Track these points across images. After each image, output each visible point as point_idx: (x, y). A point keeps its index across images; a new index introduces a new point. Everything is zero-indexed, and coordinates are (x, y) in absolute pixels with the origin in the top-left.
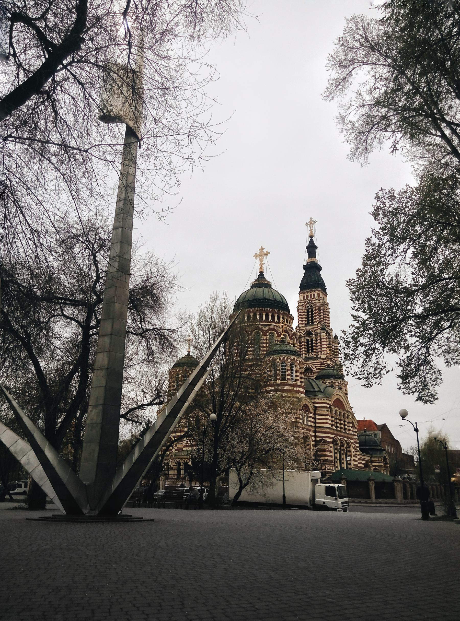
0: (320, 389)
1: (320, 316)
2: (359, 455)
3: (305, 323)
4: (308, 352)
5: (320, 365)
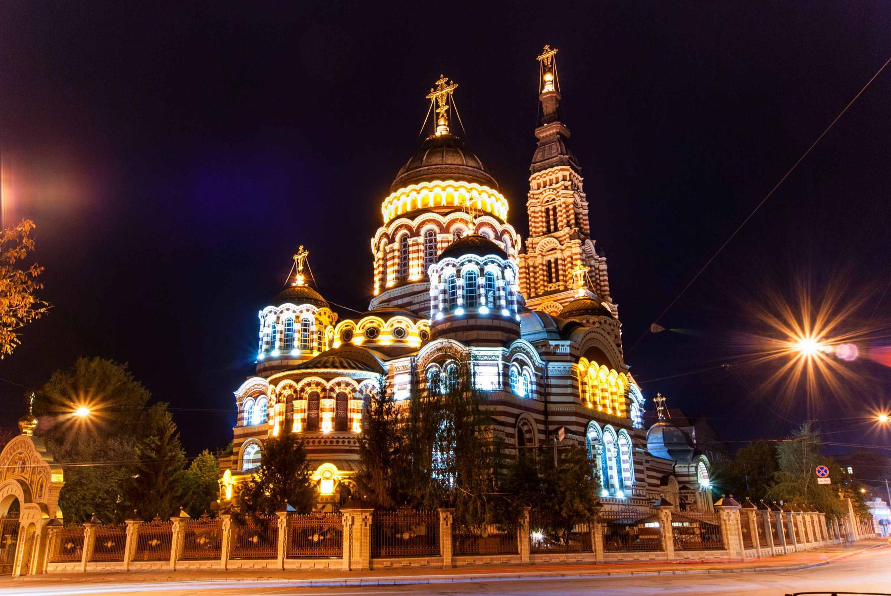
1: (567, 211)
3: (543, 232)
4: (550, 282)
5: (571, 302)
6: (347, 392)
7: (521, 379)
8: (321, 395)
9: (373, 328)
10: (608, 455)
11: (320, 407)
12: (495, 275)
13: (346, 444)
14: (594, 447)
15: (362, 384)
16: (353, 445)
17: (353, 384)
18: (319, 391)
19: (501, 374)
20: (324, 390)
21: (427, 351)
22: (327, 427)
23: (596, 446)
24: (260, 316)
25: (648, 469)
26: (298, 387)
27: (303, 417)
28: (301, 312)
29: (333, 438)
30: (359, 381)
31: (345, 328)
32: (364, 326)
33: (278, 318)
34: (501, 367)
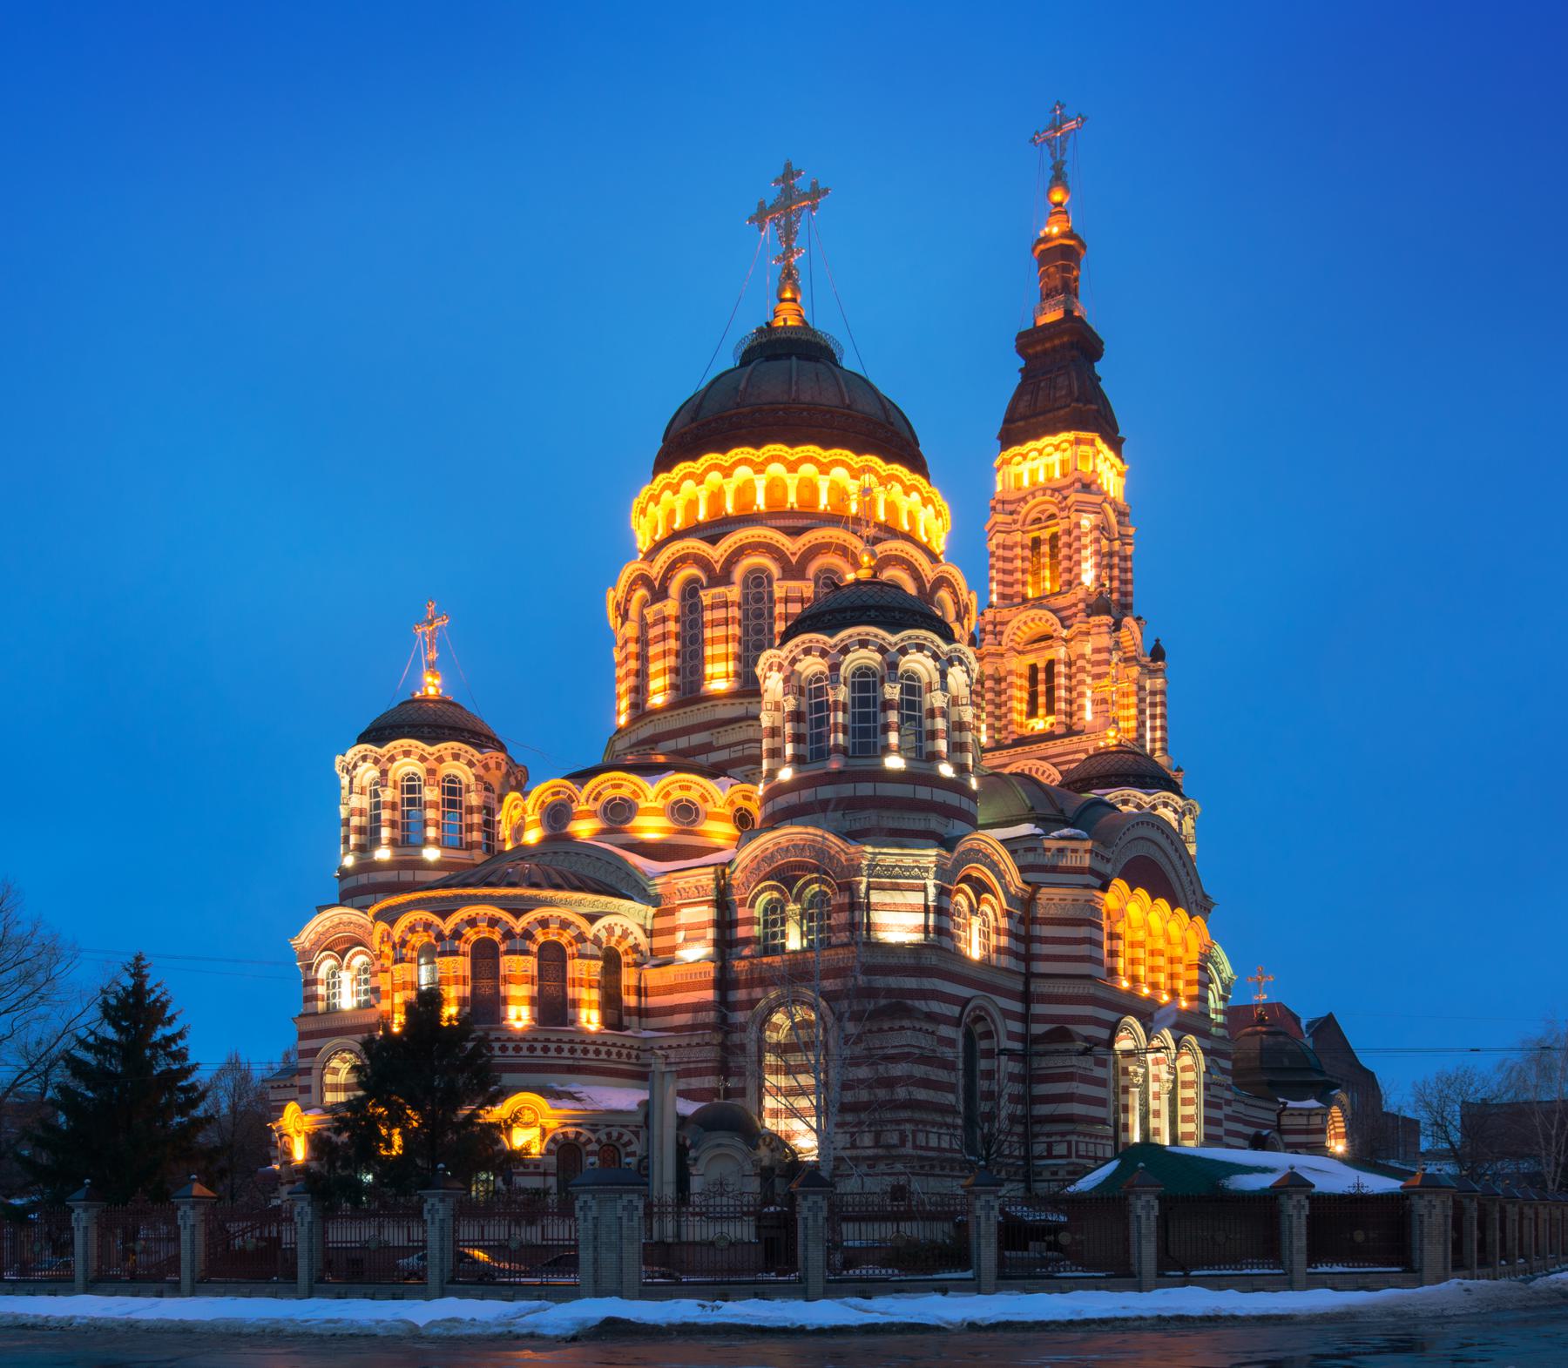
0: (1062, 811)
2: (1228, 1103)
6: (563, 941)
7: (976, 922)
8: (502, 948)
9: (621, 799)
10: (1154, 1087)
11: (502, 973)
12: (925, 679)
13: (566, 1054)
14: (1126, 1072)
15: (600, 924)
16: (582, 1056)
17: (577, 923)
18: (497, 937)
19: (931, 909)
20: (509, 934)
21: (754, 854)
22: (519, 1016)
23: (1131, 1069)
24: (338, 769)
25: (1228, 1118)
26: (447, 927)
27: (461, 995)
28: (440, 760)
29: (535, 1040)
30: (592, 918)
31: (550, 799)
32: (599, 794)
33: (384, 773)
34: (932, 891)
